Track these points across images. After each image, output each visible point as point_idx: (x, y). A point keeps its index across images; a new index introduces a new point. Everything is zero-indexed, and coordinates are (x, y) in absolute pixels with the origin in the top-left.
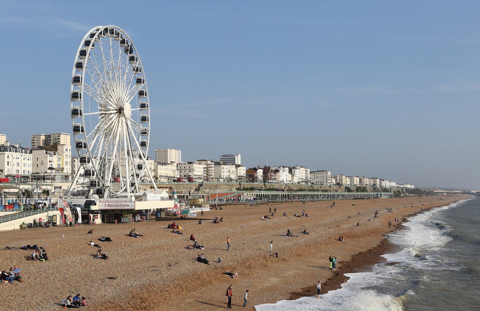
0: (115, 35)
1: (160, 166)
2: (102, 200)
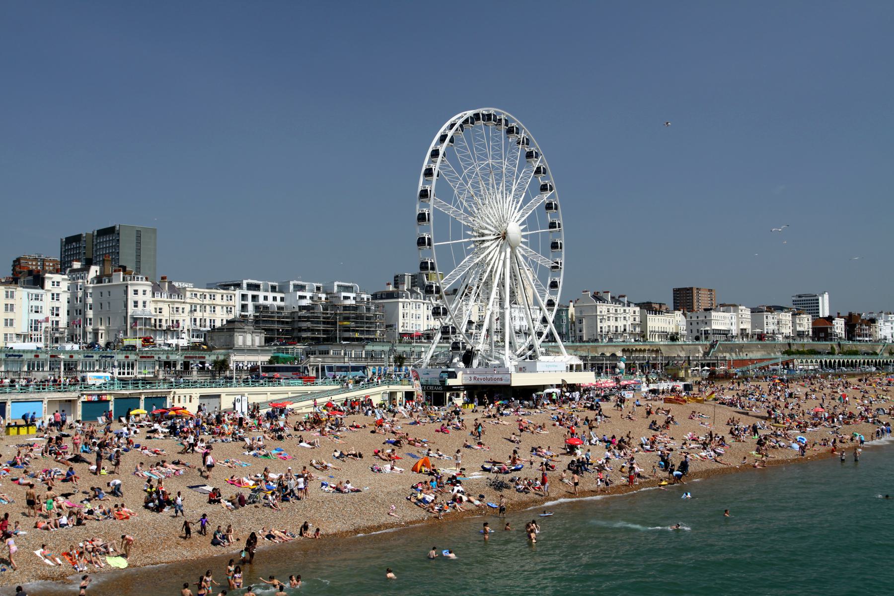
0: (494, 122)
1: (651, 315)
2: (468, 370)
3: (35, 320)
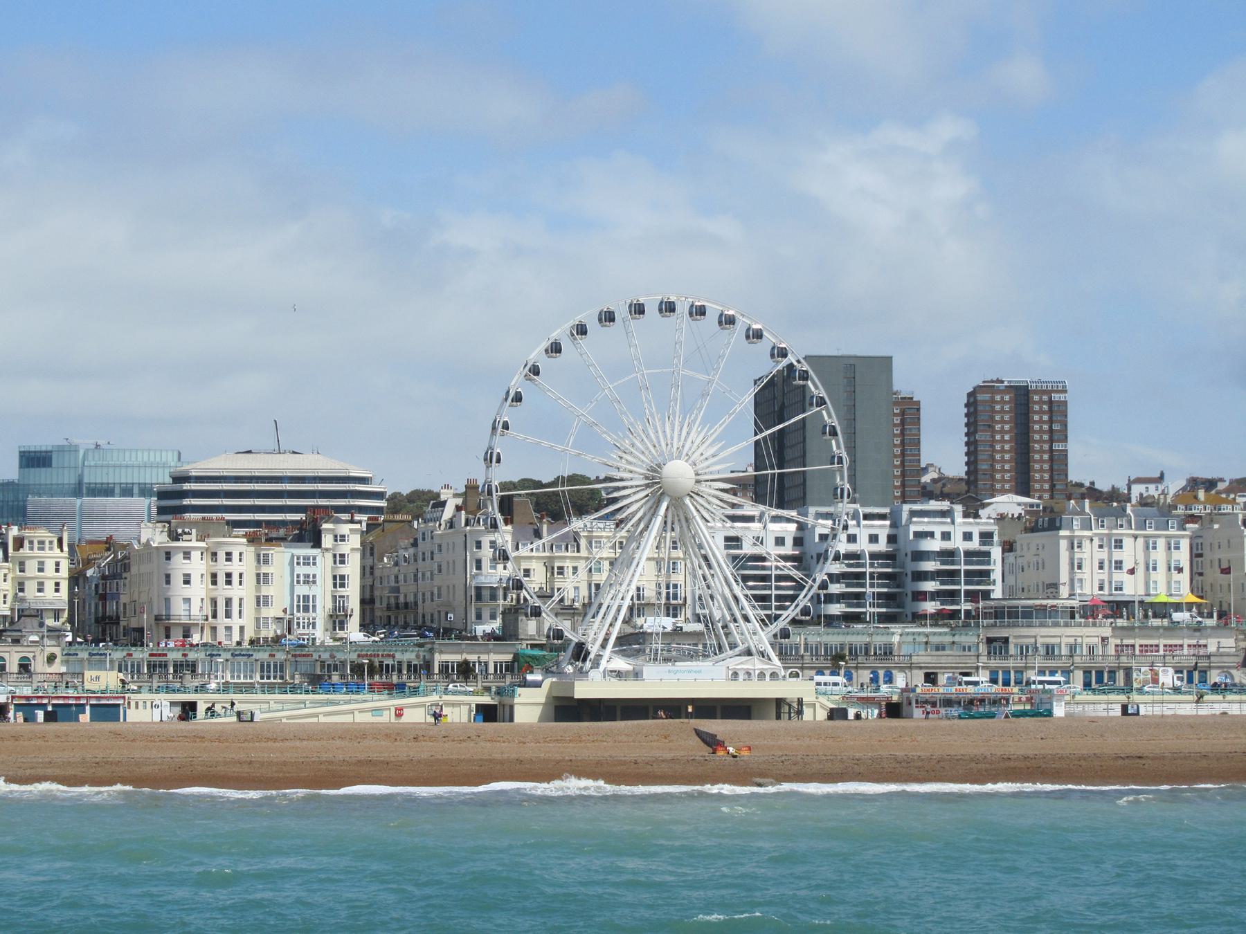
3: (304, 596)
